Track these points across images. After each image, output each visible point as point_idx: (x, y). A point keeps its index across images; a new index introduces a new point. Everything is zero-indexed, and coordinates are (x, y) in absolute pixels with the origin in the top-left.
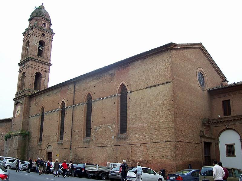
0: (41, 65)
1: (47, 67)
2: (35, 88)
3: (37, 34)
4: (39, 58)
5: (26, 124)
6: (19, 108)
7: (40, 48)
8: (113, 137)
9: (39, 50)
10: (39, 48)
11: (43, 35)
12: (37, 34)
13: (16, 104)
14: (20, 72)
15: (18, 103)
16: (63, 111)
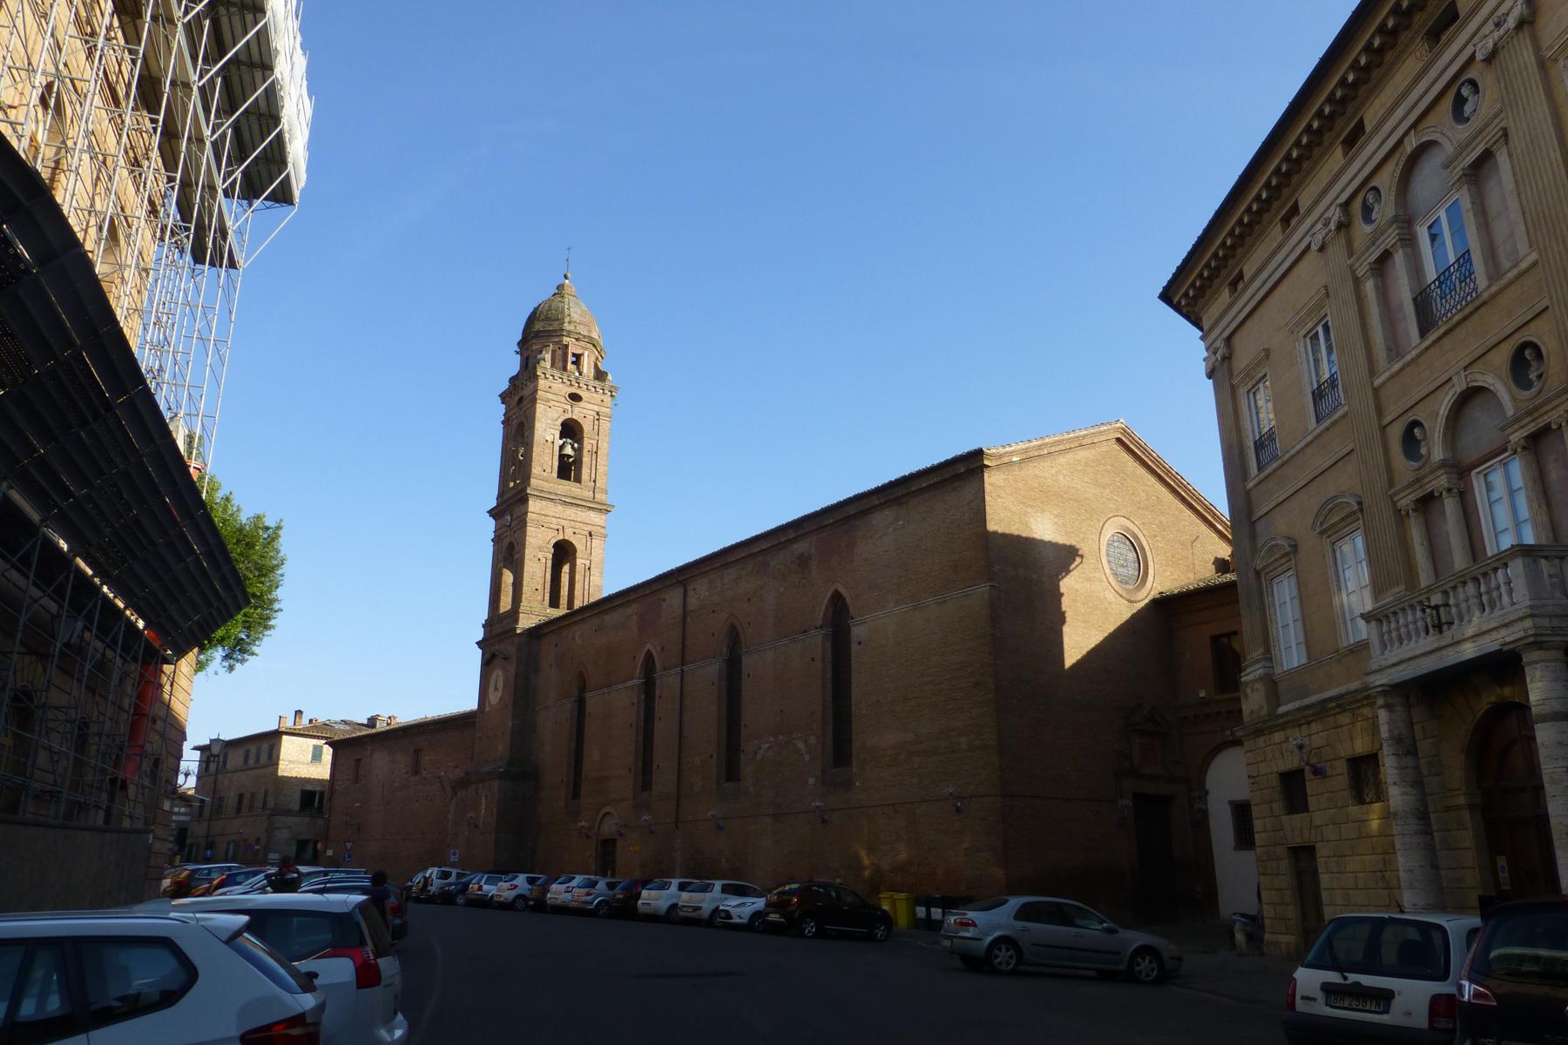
0: (571, 512)
1: (594, 517)
2: (554, 602)
3: (550, 396)
4: (566, 487)
5: (524, 731)
6: (498, 675)
7: (568, 450)
8: (812, 781)
9: (562, 457)
10: (562, 448)
11: (575, 398)
12: (550, 396)
13: (487, 664)
14: (497, 540)
15: (493, 656)
16: (649, 685)
